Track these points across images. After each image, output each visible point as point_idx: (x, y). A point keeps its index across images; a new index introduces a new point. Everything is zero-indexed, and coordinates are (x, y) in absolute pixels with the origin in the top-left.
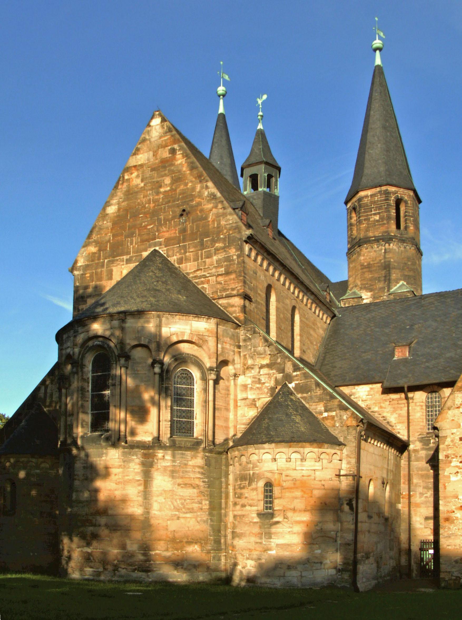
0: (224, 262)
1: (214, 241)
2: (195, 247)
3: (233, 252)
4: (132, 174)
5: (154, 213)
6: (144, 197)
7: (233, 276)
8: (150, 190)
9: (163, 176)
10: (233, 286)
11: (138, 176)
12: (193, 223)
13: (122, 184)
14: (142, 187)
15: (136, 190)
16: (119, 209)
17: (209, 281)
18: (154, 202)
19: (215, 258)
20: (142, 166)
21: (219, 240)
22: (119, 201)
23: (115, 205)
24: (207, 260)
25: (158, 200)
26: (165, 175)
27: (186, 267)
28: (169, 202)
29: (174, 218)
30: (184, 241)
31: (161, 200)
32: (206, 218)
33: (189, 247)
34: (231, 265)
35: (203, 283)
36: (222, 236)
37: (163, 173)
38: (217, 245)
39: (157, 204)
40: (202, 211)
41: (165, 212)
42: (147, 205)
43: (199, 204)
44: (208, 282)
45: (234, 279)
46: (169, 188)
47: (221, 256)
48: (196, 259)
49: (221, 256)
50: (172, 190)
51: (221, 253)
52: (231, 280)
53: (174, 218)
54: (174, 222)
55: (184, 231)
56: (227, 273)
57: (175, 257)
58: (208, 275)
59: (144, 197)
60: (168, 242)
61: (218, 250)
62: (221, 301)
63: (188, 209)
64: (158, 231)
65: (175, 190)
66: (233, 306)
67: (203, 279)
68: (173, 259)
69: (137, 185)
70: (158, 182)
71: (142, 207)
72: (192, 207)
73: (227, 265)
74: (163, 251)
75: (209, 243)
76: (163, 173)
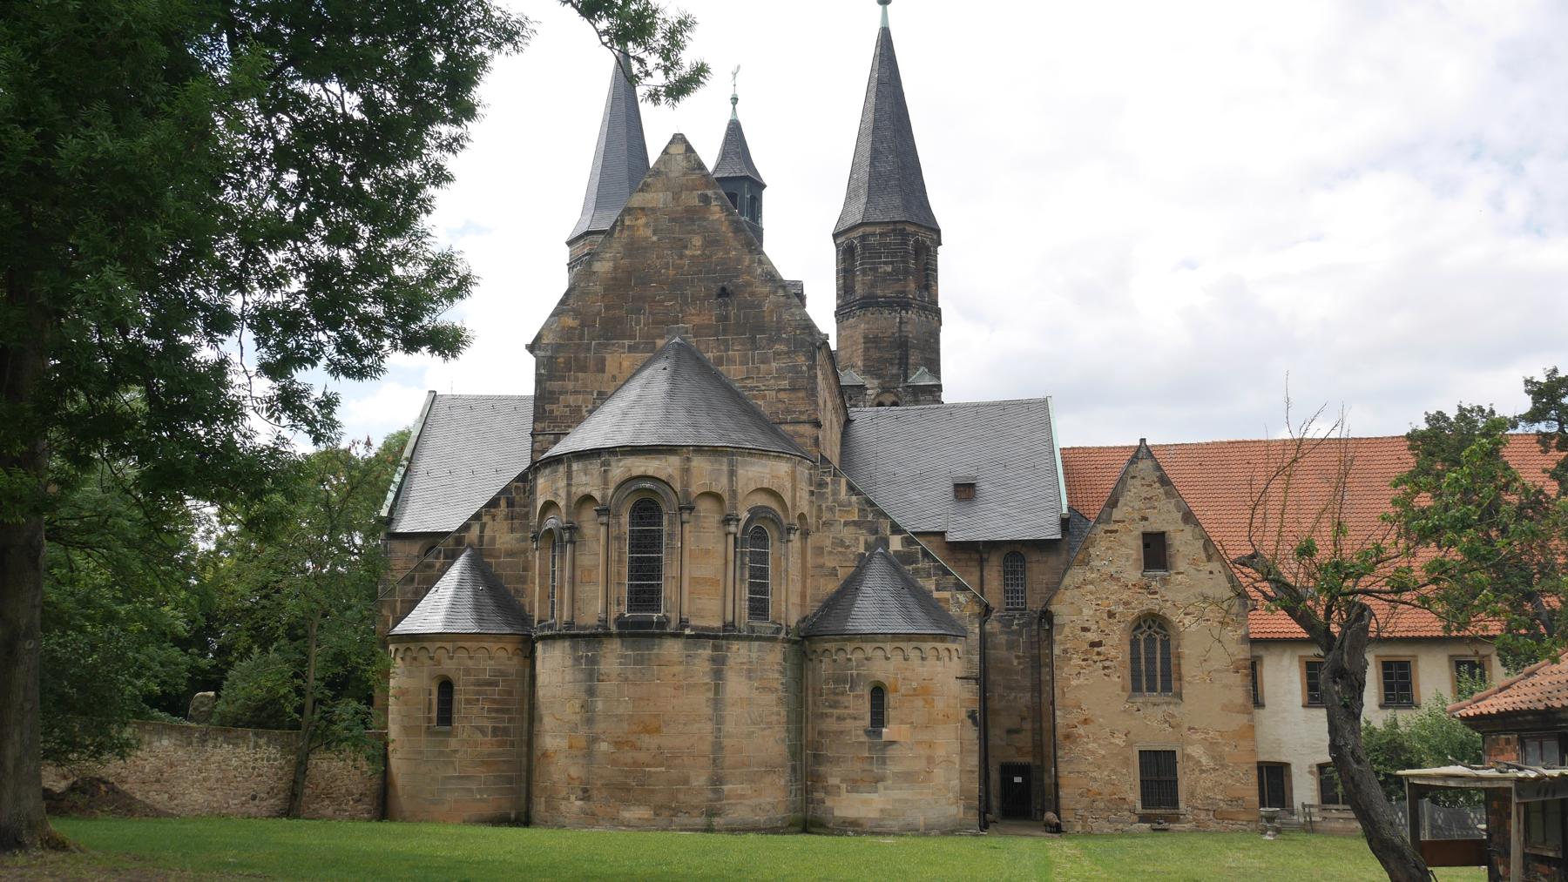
1: (771, 341)
3: (801, 360)
4: (637, 219)
6: (657, 258)
7: (802, 394)
9: (689, 233)
11: (647, 225)
13: (621, 231)
14: (653, 243)
15: (644, 244)
17: (765, 396)
18: (674, 269)
19: (774, 365)
20: (653, 210)
21: (779, 340)
22: (615, 256)
24: (762, 366)
27: (729, 371)
28: (700, 272)
29: (708, 297)
30: (725, 332)
32: (760, 306)
35: (755, 397)
36: (784, 336)
40: (752, 294)
41: (694, 286)
43: (748, 284)
44: (764, 397)
45: (803, 399)
47: (782, 363)
48: (744, 362)
49: (782, 363)
53: (708, 297)
56: (793, 389)
57: (711, 355)
58: (763, 388)
59: (657, 258)
61: (779, 355)
63: (731, 288)
64: (681, 311)
65: (710, 257)
66: (802, 436)
74: (693, 341)
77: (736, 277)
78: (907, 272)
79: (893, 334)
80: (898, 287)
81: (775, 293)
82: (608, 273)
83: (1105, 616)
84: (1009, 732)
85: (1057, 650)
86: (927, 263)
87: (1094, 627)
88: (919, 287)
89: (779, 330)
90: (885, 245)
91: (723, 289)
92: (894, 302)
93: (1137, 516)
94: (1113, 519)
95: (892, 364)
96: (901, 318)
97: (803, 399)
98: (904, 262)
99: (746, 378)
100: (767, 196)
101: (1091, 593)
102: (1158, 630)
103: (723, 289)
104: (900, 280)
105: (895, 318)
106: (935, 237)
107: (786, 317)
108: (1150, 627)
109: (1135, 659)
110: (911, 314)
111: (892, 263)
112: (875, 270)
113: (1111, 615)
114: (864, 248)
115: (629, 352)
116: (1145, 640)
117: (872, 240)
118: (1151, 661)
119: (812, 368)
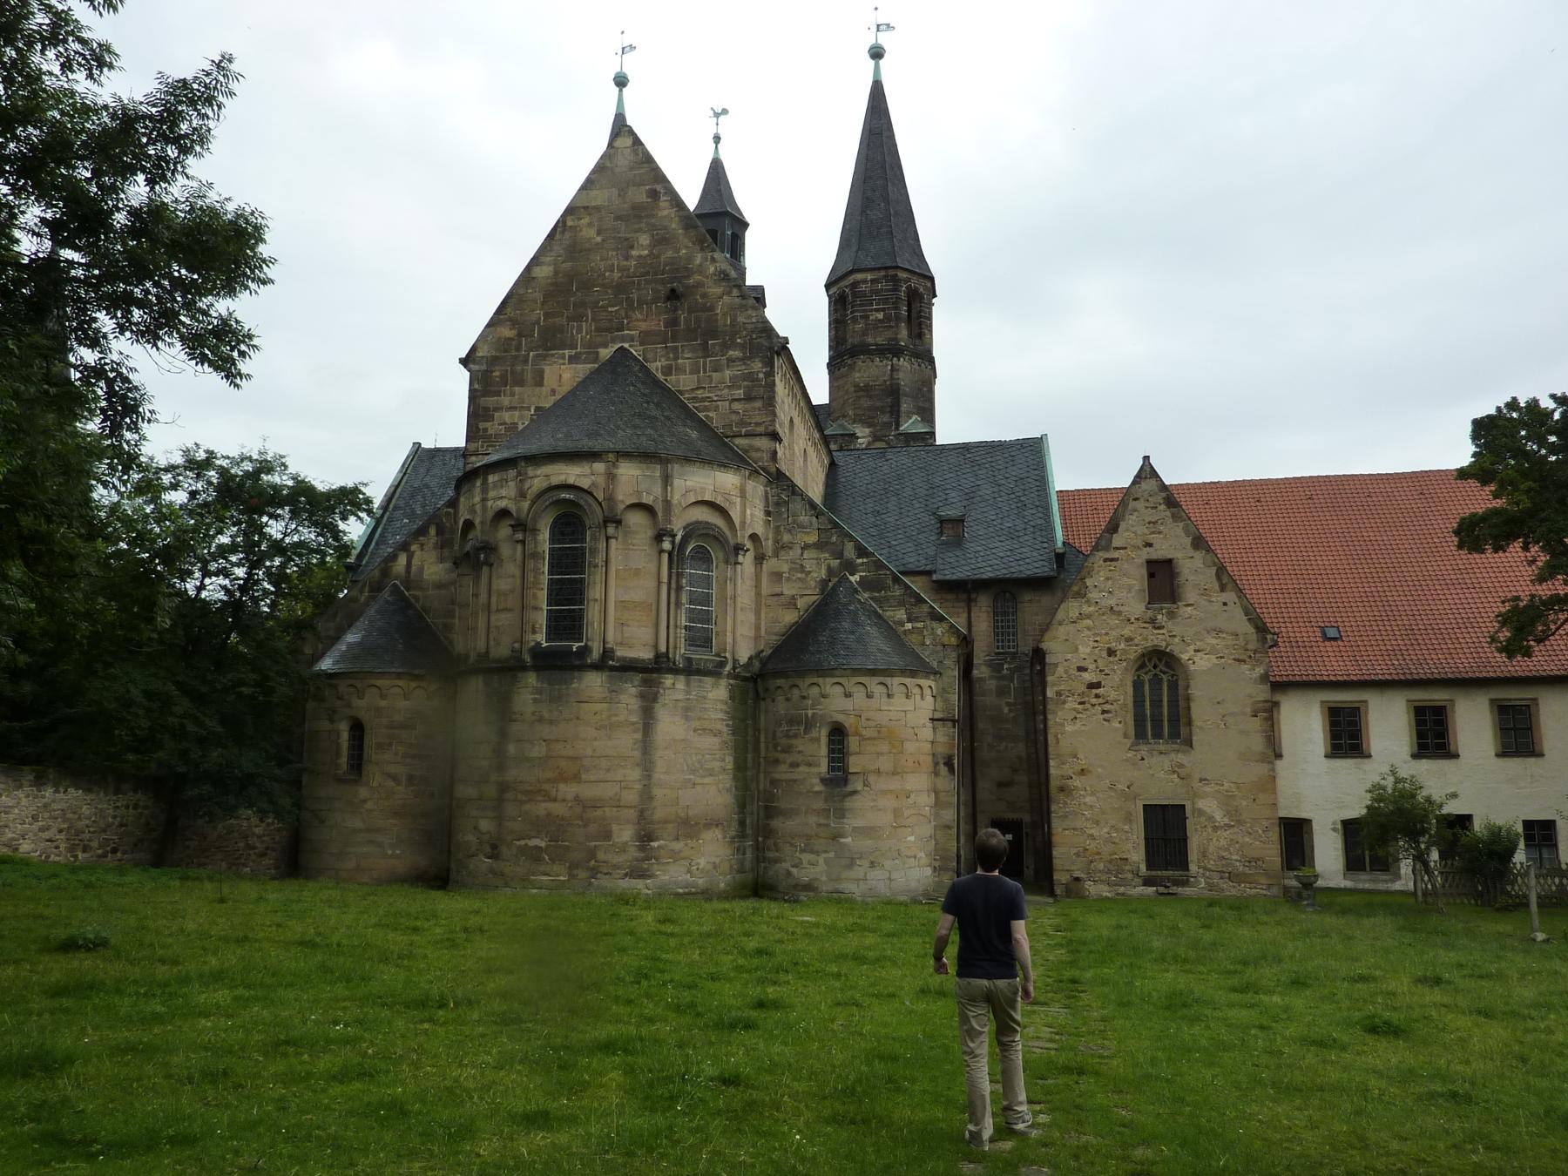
0: (745, 380)
1: (725, 347)
2: (694, 351)
3: (757, 366)
4: (580, 219)
5: (620, 288)
6: (601, 260)
7: (758, 404)
8: (613, 250)
9: (637, 232)
10: (758, 419)
11: (590, 225)
12: (689, 313)
13: (563, 232)
14: (597, 244)
15: (587, 245)
16: (556, 273)
17: (717, 407)
19: (728, 373)
20: (598, 209)
21: (734, 346)
23: (549, 265)
24: (714, 374)
25: (626, 269)
26: (640, 230)
27: (678, 380)
28: (647, 273)
29: (655, 300)
30: (674, 338)
31: (632, 270)
32: (712, 309)
33: (683, 351)
34: (755, 386)
35: (706, 409)
36: (739, 340)
37: (637, 226)
38: (731, 353)
39: (625, 273)
40: (704, 296)
42: (607, 274)
43: (699, 285)
44: (716, 409)
46: (646, 252)
47: (738, 370)
48: (696, 371)
49: (738, 370)
50: (651, 254)
51: (737, 366)
52: (754, 409)
53: (655, 300)
54: (656, 306)
55: (673, 323)
56: (748, 398)
57: (658, 364)
58: (715, 398)
59: (601, 260)
60: (645, 338)
62: (738, 441)
64: (627, 317)
65: (658, 257)
67: (706, 404)
68: (656, 367)
69: (590, 239)
70: (627, 239)
71: (599, 276)
72: (687, 287)
73: (747, 387)
75: (717, 347)
76: (637, 226)
77: (685, 277)
78: (898, 318)
79: (885, 381)
80: (889, 334)
81: (729, 293)
82: (548, 278)
83: (1105, 654)
84: (1001, 785)
85: (1050, 693)
86: (920, 312)
87: (1092, 667)
88: (910, 335)
89: (734, 335)
90: (877, 292)
91: (673, 291)
92: (886, 349)
93: (1140, 544)
94: (1113, 545)
95: (883, 413)
96: (892, 366)
97: (759, 410)
98: (896, 308)
99: (698, 389)
100: (750, 237)
101: (1089, 629)
102: (1163, 669)
103: (673, 291)
104: (892, 327)
105: (887, 365)
106: (929, 285)
107: (740, 319)
108: (1155, 667)
109: (1138, 702)
110: (903, 363)
111: (883, 310)
112: (867, 317)
113: (1111, 652)
114: (855, 295)
115: (570, 363)
116: (1150, 680)
117: (863, 287)
118: (1156, 704)
119: (770, 374)
